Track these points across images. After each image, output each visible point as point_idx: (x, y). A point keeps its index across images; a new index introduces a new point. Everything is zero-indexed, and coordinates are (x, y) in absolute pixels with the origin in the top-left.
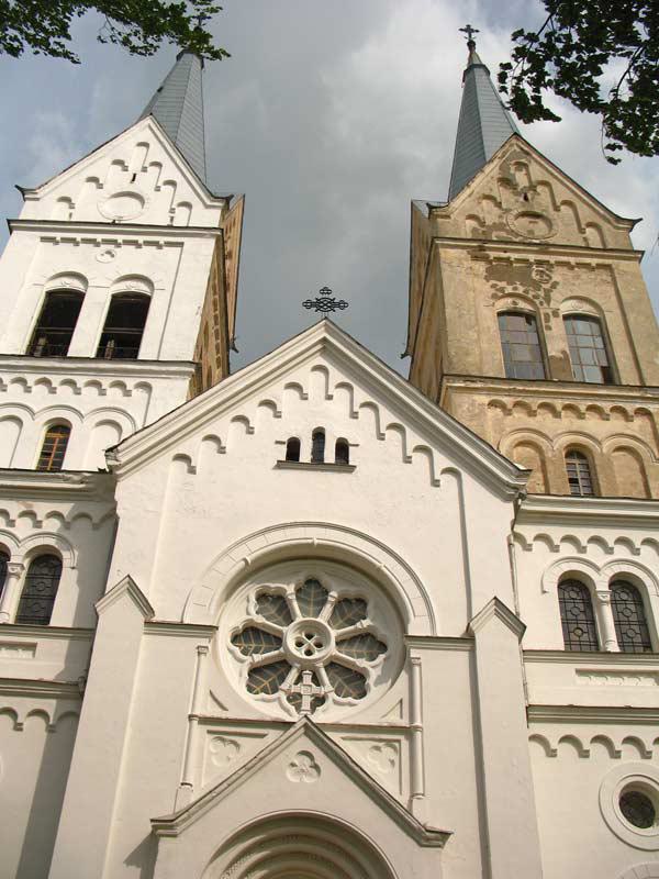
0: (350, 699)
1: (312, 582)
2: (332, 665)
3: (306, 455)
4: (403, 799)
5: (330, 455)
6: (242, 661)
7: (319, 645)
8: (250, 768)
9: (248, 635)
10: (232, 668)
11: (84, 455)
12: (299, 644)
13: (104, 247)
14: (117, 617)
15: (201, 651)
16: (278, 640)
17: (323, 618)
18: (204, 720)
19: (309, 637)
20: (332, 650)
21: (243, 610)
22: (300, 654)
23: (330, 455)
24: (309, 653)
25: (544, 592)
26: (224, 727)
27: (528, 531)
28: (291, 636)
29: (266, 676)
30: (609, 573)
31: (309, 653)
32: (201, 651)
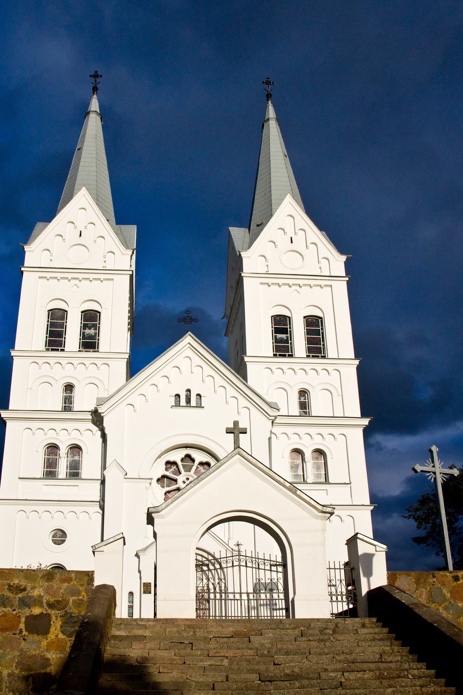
13: (73, 282)
23: (193, 403)
25: (283, 458)
28: (180, 479)
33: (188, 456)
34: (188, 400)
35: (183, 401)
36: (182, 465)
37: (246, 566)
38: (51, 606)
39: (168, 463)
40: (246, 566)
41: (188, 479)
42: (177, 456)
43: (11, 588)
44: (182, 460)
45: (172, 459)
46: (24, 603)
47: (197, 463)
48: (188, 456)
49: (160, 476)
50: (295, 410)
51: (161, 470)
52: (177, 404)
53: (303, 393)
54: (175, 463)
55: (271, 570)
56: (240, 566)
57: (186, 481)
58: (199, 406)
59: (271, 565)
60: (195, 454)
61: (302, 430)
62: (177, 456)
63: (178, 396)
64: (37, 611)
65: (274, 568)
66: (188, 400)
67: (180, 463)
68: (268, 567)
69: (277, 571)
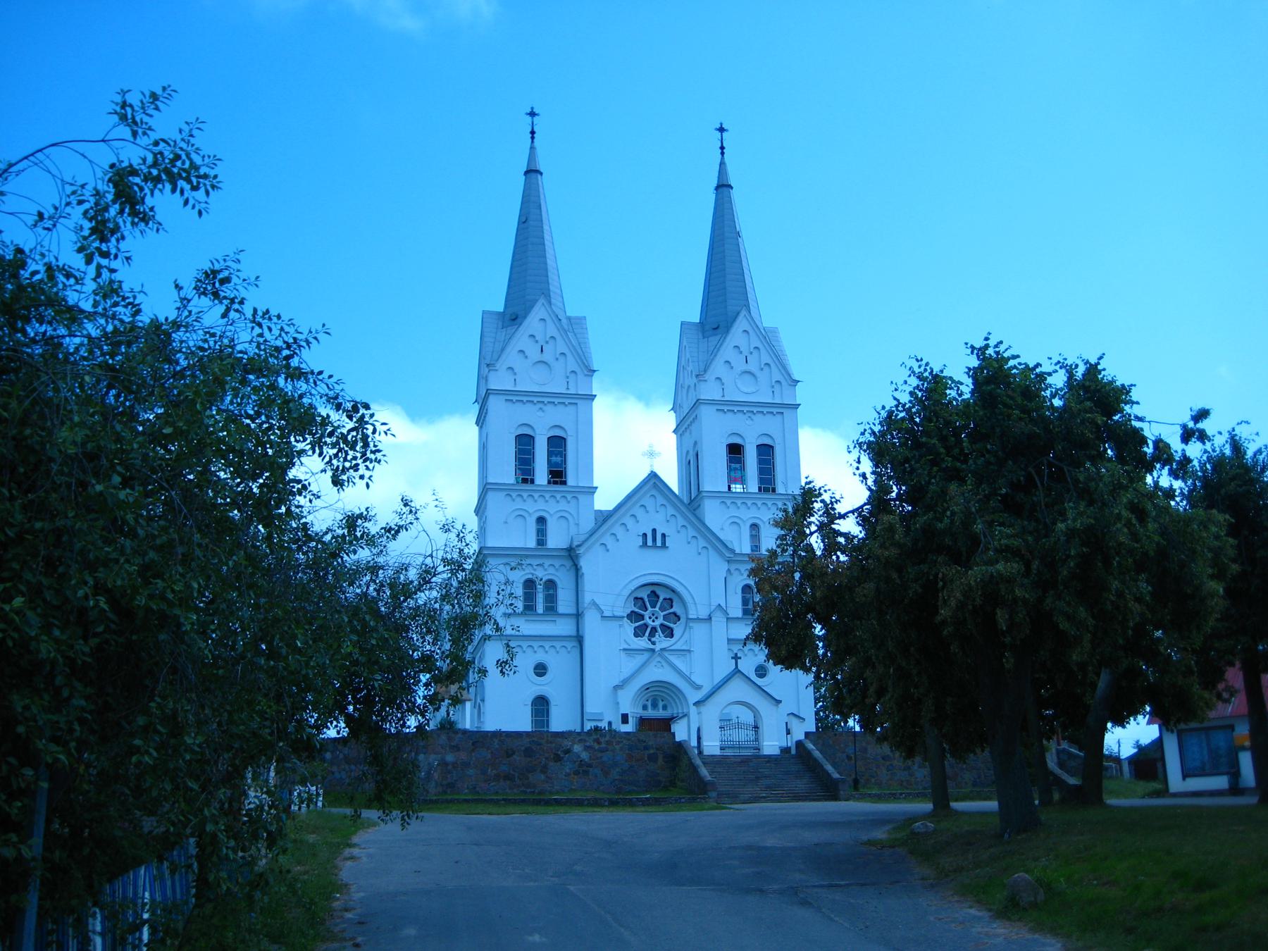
1: (653, 592)
2: (662, 625)
3: (650, 543)
4: (688, 674)
5: (659, 543)
8: (644, 665)
9: (634, 616)
10: (629, 628)
11: (556, 540)
12: (650, 618)
15: (620, 626)
16: (642, 617)
17: (657, 609)
18: (625, 650)
19: (653, 615)
22: (650, 622)
26: (628, 651)
27: (733, 567)
28: (647, 614)
29: (639, 632)
31: (653, 621)
32: (620, 626)
34: (654, 539)
35: (650, 543)
38: (657, 749)
39: (636, 598)
41: (653, 615)
42: (644, 594)
43: (639, 740)
45: (639, 596)
46: (646, 748)
47: (661, 599)
48: (653, 592)
51: (631, 607)
52: (645, 544)
54: (642, 599)
58: (664, 545)
60: (659, 591)
62: (644, 594)
63: (645, 535)
64: (652, 751)
66: (654, 539)
67: (646, 600)
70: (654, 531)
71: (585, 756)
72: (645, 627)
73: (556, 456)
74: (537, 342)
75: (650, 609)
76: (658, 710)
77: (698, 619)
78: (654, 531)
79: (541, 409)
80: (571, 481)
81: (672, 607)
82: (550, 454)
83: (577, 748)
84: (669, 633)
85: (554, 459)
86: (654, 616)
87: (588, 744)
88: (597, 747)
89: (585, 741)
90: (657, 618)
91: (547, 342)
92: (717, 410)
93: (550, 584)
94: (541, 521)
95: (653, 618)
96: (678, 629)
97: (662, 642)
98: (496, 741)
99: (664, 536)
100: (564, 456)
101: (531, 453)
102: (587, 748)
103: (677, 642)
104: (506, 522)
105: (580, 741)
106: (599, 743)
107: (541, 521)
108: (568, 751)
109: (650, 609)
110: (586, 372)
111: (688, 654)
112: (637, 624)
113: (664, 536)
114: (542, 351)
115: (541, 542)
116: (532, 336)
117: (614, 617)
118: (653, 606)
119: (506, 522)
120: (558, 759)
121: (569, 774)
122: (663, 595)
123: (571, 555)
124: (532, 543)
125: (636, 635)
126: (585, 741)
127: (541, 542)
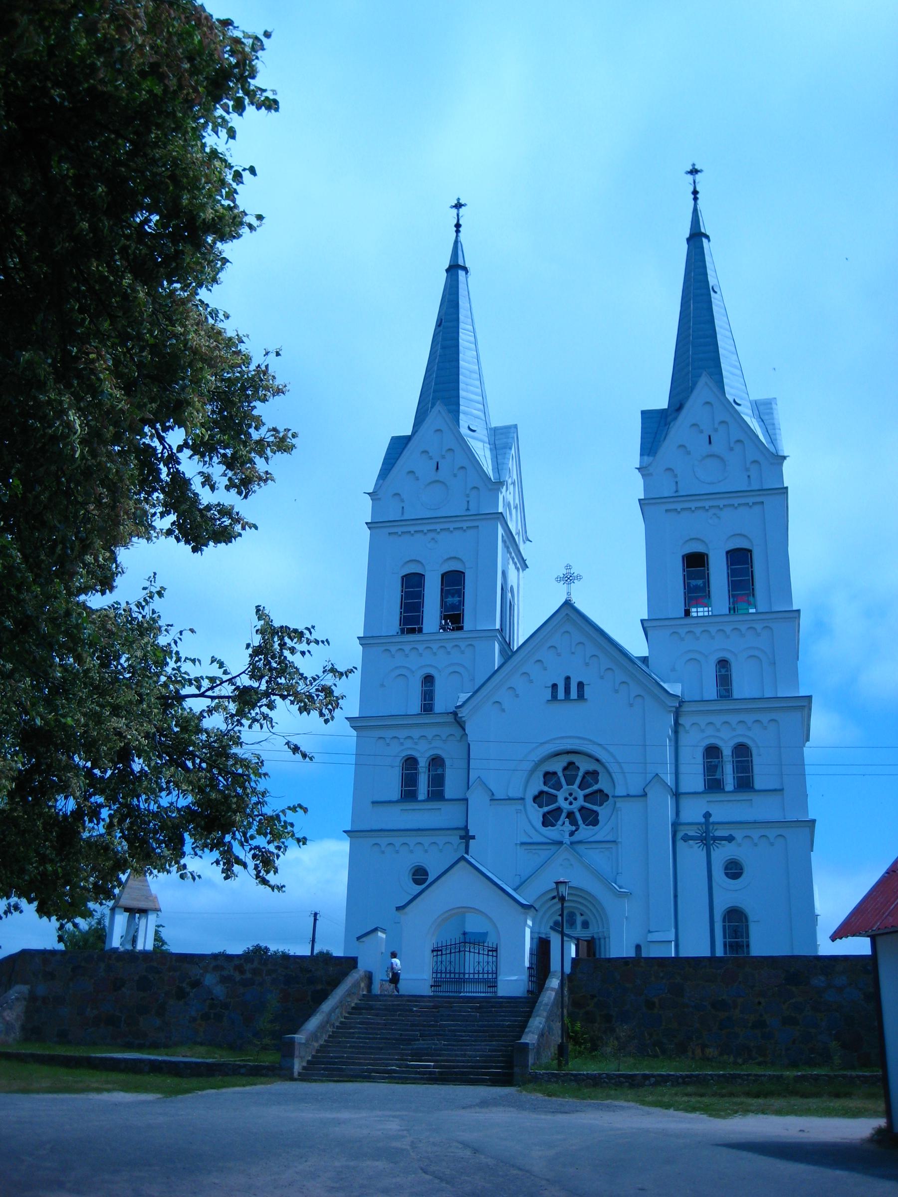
0: (591, 827)
2: (582, 809)
6: (539, 811)
7: (575, 799)
10: (536, 813)
12: (566, 799)
13: (430, 535)
14: (477, 798)
17: (575, 787)
20: (581, 802)
21: (537, 785)
24: (571, 803)
28: (561, 795)
30: (732, 743)
31: (571, 803)
33: (571, 764)
36: (549, 787)
37: (470, 951)
40: (470, 951)
41: (571, 794)
42: (557, 766)
44: (545, 783)
48: (571, 764)
49: (536, 793)
50: (711, 690)
53: (723, 663)
54: (555, 773)
55: (488, 955)
56: (465, 951)
57: (569, 797)
59: (488, 951)
60: (579, 761)
61: (718, 720)
62: (557, 766)
65: (490, 953)
67: (560, 774)
68: (486, 953)
69: (493, 956)
70: (568, 679)
71: (219, 991)
72: (583, 811)
73: (453, 597)
74: (431, 458)
75: (565, 786)
76: (576, 928)
77: (628, 796)
78: (568, 679)
79: (433, 539)
80: (467, 624)
81: (597, 782)
82: (444, 594)
83: (210, 979)
84: (592, 819)
85: (450, 600)
86: (571, 798)
87: (225, 973)
88: (238, 977)
89: (222, 968)
90: (575, 799)
91: (443, 457)
92: (666, 511)
93: (437, 762)
94: (429, 680)
95: (571, 799)
96: (603, 811)
97: (585, 832)
98: (102, 965)
99: (581, 685)
100: (460, 593)
101: (420, 595)
102: (224, 980)
103: (601, 832)
104: (382, 686)
105: (217, 968)
106: (242, 972)
107: (429, 680)
108: (196, 984)
109: (565, 786)
110: (490, 487)
111: (613, 846)
112: (546, 809)
113: (581, 685)
114: (437, 468)
115: (427, 707)
116: (425, 452)
117: (510, 799)
118: (570, 782)
119: (382, 686)
120: (181, 995)
121: (194, 1020)
122: (584, 766)
123: (457, 720)
124: (415, 706)
125: (544, 824)
126: (222, 968)
127: (427, 707)
